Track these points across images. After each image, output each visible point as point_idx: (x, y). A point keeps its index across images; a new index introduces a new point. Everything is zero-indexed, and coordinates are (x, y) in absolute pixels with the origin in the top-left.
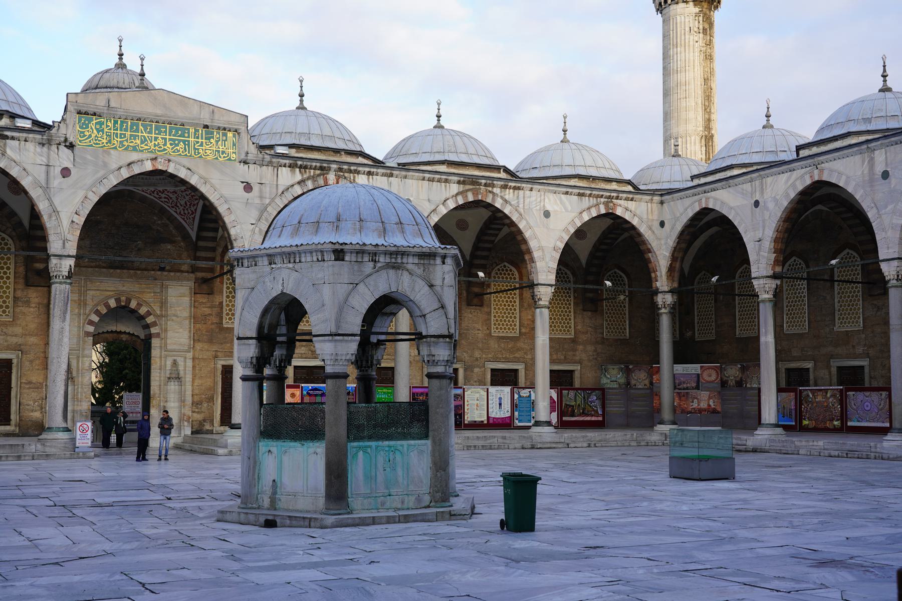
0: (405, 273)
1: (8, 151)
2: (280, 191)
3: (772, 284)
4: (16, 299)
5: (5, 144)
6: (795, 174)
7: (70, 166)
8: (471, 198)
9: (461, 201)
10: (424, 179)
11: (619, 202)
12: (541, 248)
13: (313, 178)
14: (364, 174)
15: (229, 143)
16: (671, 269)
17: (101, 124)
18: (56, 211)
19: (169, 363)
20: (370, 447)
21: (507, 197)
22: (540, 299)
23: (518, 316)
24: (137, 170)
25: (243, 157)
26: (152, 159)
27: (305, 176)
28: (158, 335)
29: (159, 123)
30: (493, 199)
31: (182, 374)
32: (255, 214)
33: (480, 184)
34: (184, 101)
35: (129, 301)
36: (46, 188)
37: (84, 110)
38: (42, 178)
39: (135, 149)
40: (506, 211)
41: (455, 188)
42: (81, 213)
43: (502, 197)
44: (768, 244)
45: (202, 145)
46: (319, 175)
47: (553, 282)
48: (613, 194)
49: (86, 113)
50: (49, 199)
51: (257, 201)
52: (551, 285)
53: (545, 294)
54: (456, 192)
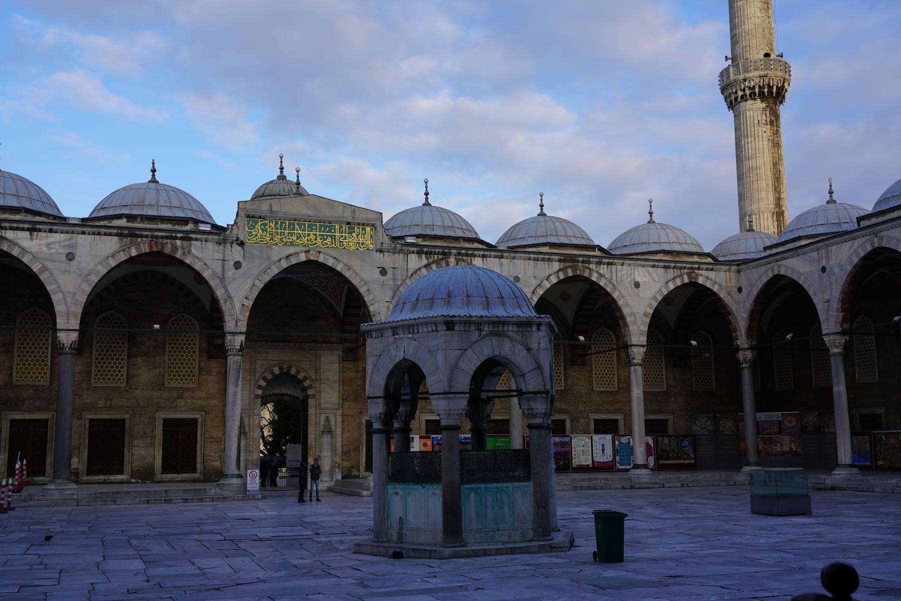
0: (507, 340)
1: (193, 250)
2: (410, 274)
3: (842, 340)
4: (200, 369)
5: (190, 245)
6: (857, 243)
7: (241, 260)
8: (570, 273)
9: (562, 276)
10: (530, 259)
11: (700, 272)
12: (633, 314)
13: (437, 262)
15: (367, 236)
16: (749, 330)
18: (230, 297)
19: (323, 419)
20: (480, 488)
21: (601, 272)
22: (634, 358)
24: (294, 261)
25: (379, 246)
26: (306, 252)
28: (313, 396)
29: (311, 222)
30: (590, 274)
31: (333, 427)
32: (389, 293)
33: (578, 262)
34: (331, 203)
35: (289, 368)
36: (222, 279)
37: (251, 214)
38: (219, 270)
39: (292, 244)
40: (602, 283)
41: (556, 266)
42: (250, 297)
43: (597, 272)
44: (835, 304)
45: (345, 238)
46: (442, 259)
49: (253, 217)
50: (225, 288)
51: (391, 282)
52: (643, 346)
53: (638, 354)
54: (557, 269)
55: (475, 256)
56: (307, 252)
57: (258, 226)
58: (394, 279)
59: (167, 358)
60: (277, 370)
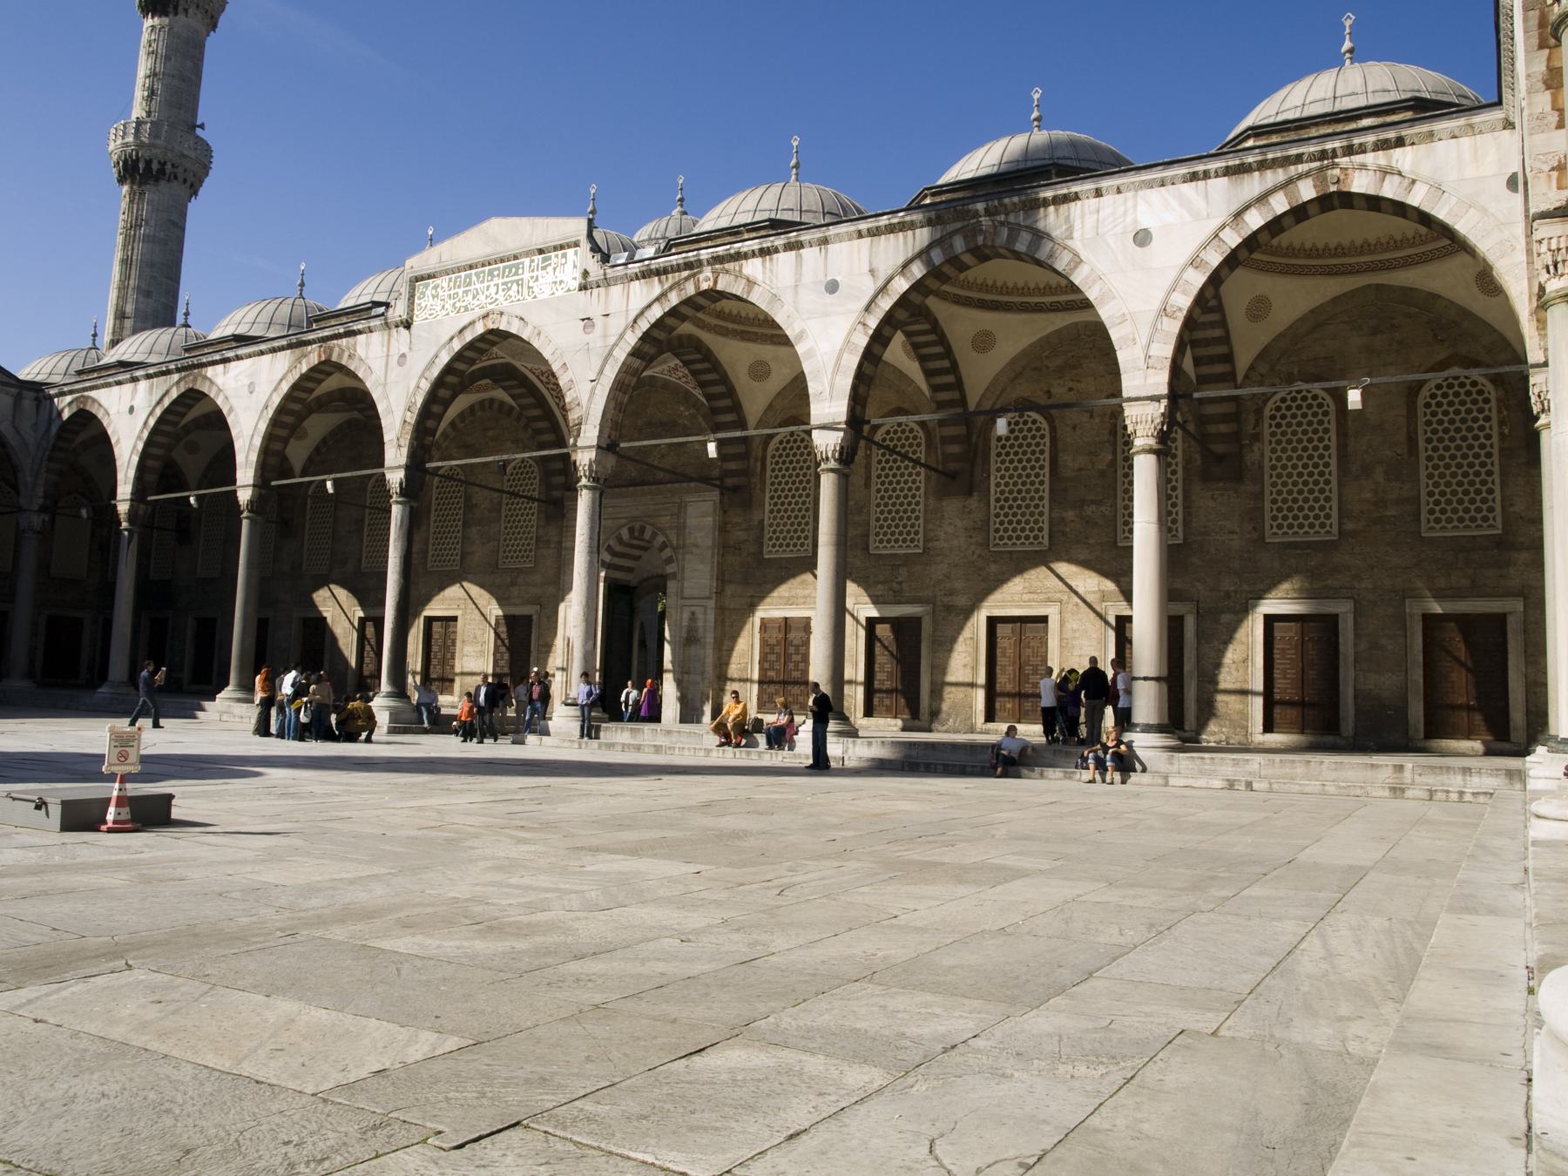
1: (360, 351)
7: (405, 350)
10: (860, 235)
11: (1358, 159)
14: (754, 254)
15: (569, 266)
17: (436, 287)
19: (686, 616)
23: (1334, 496)
24: (469, 336)
28: (674, 576)
33: (976, 214)
35: (643, 529)
39: (466, 309)
46: (687, 279)
47: (1164, 390)
48: (1329, 146)
52: (1156, 398)
55: (745, 256)
56: (485, 317)
58: (605, 336)
60: (625, 533)
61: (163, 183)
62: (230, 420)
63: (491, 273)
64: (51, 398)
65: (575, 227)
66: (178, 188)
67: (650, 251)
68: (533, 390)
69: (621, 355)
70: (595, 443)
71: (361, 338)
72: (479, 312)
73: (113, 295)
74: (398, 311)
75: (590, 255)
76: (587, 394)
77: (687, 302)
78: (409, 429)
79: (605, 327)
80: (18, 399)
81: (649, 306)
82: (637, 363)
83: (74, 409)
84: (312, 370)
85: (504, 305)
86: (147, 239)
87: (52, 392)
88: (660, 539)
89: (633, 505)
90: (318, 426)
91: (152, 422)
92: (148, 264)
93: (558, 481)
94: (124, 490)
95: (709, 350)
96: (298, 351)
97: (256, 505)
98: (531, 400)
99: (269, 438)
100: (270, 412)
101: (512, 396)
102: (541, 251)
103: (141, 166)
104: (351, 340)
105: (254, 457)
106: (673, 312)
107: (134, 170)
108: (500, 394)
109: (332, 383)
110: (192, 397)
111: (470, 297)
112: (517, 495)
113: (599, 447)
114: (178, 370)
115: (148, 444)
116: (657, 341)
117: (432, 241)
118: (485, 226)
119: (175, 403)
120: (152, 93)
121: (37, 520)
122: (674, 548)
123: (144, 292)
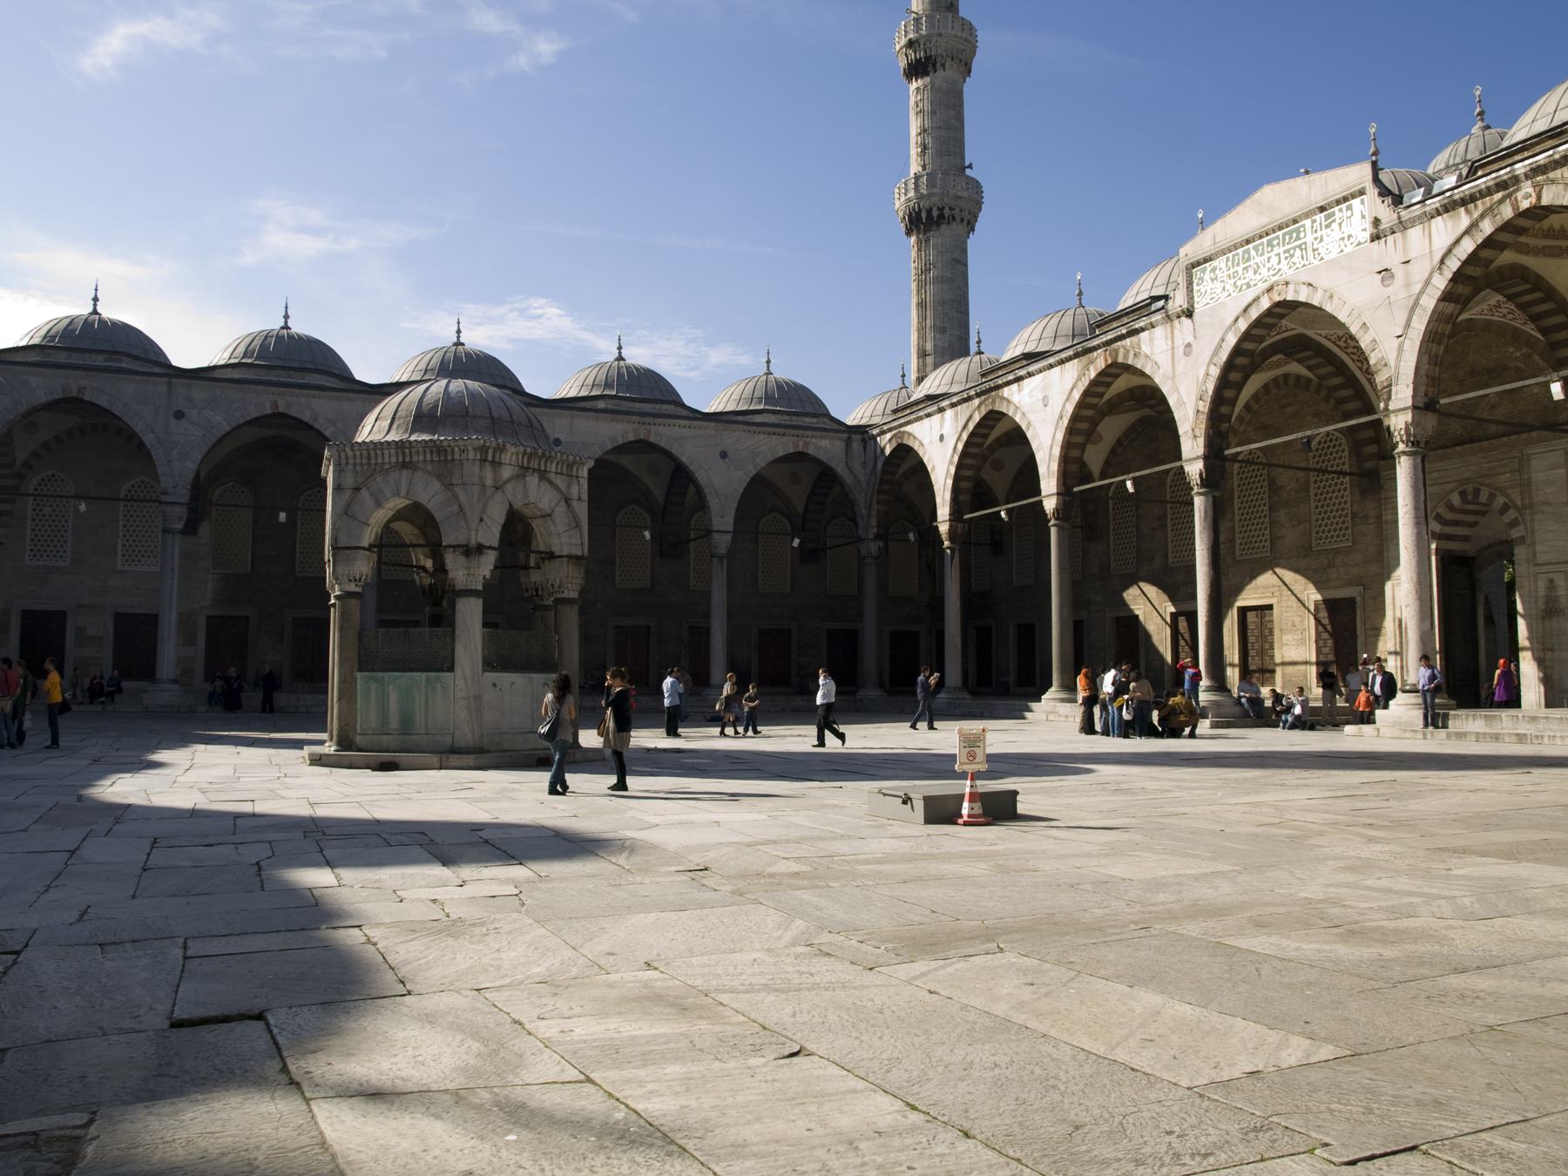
1: (1145, 349)
4: (1354, 515)
7: (1190, 339)
15: (1357, 215)
17: (1213, 270)
18: (1182, 403)
19: (1542, 584)
24: (1254, 314)
27: (1476, 215)
32: (1401, 317)
35: (1477, 492)
39: (1249, 286)
46: (1501, 201)
50: (1177, 390)
56: (1270, 290)
57: (1207, 276)
58: (1408, 285)
59: (1313, 505)
60: (1456, 499)
61: (943, 226)
62: (1029, 435)
63: (1270, 243)
64: (874, 438)
65: (1359, 174)
66: (957, 228)
67: (1451, 180)
68: (1330, 358)
69: (1429, 302)
70: (1410, 403)
71: (1144, 335)
72: (1263, 286)
73: (914, 337)
74: (1178, 302)
75: (1379, 200)
76: (1393, 348)
77: (1506, 227)
78: (1203, 418)
79: (1407, 275)
80: (848, 442)
81: (1457, 242)
82: (1450, 308)
83: (894, 444)
84: (1100, 374)
85: (1287, 272)
86: (936, 280)
87: (875, 432)
88: (1500, 500)
89: (1459, 467)
90: (1112, 428)
91: (960, 447)
92: (940, 303)
93: (1373, 450)
94: (943, 512)
95: (1539, 277)
96: (1084, 359)
97: (1062, 512)
98: (1330, 369)
99: (1067, 446)
100: (1066, 421)
101: (1309, 368)
102: (1322, 209)
103: (924, 215)
104: (1134, 339)
105: (1055, 467)
106: (1489, 243)
107: (920, 221)
108: (1295, 368)
109: (1122, 384)
110: (993, 418)
111: (1251, 272)
112: (1325, 471)
113: (1415, 407)
114: (978, 395)
115: (959, 467)
116: (1471, 280)
117: (1203, 225)
118: (1257, 196)
119: (978, 425)
120: (924, 147)
121: (874, 548)
122: (1517, 508)
123: (940, 329)
